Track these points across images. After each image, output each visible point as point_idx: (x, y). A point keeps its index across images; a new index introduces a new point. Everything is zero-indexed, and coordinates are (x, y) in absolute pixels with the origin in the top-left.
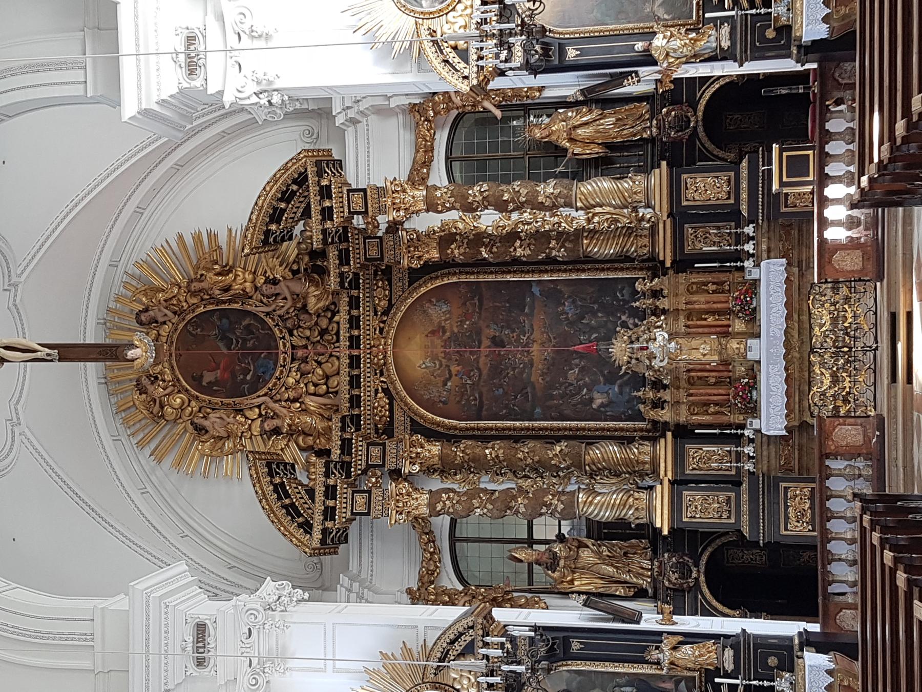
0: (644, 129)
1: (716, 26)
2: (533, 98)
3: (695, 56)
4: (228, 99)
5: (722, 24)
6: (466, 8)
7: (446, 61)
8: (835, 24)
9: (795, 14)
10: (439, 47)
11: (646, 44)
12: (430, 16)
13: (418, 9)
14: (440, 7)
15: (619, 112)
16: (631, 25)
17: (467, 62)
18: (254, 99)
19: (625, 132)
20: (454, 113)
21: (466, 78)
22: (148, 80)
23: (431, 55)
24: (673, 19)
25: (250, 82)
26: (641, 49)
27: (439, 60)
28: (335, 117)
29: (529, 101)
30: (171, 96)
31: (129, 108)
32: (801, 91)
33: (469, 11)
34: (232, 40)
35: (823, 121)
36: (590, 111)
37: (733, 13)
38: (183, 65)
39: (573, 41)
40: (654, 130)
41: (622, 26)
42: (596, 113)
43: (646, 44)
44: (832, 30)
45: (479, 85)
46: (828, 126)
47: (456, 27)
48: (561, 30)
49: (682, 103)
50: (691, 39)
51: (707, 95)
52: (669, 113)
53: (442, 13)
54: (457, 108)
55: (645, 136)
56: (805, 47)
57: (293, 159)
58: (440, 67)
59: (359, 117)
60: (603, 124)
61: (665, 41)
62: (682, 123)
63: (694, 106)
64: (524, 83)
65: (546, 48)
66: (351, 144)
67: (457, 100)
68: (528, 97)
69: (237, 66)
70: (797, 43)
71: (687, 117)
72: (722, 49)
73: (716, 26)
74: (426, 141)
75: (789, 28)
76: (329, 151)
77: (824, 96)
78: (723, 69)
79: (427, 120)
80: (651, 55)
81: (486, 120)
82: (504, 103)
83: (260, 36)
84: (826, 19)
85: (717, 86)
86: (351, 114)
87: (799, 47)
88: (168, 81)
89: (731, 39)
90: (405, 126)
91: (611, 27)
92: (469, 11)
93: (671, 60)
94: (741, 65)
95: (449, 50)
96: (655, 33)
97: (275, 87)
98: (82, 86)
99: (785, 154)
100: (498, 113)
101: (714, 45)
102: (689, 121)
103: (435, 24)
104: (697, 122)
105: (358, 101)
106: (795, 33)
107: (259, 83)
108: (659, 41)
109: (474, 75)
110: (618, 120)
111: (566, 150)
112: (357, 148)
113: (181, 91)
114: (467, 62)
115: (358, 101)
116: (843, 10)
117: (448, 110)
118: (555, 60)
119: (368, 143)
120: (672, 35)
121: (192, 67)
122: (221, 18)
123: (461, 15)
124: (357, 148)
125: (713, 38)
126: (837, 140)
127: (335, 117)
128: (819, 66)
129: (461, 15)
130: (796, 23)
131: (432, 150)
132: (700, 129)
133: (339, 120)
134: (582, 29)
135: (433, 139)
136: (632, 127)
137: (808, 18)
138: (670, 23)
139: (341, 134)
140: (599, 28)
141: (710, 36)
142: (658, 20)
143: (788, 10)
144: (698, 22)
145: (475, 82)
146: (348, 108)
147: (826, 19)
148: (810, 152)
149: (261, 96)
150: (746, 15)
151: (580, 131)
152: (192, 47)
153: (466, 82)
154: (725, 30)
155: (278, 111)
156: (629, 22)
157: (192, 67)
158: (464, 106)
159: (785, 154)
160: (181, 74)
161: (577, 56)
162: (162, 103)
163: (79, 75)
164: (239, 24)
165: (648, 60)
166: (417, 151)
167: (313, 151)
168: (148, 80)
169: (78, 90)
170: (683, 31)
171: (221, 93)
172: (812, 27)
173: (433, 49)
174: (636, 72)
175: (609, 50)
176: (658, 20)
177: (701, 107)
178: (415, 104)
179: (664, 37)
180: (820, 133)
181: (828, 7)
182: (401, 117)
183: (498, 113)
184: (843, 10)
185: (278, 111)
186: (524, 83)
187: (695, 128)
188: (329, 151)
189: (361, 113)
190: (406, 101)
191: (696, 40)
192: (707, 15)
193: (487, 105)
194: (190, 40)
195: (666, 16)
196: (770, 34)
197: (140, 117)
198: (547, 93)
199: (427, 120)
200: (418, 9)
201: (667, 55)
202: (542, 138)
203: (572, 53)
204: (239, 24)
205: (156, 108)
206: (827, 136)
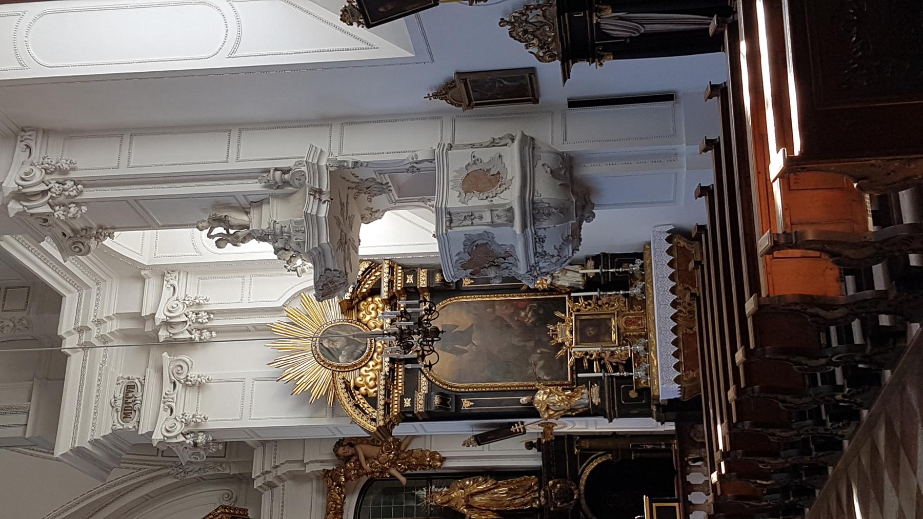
0: (534, 500)
1: (587, 386)
2: (435, 467)
3: (572, 410)
4: (157, 436)
5: (592, 384)
6: (377, 364)
7: (357, 406)
8: (686, 385)
9: (652, 378)
10: (352, 394)
11: (530, 398)
12: (345, 369)
13: (335, 364)
14: (354, 362)
15: (511, 483)
16: (517, 383)
17: (375, 407)
18: (182, 439)
19: (517, 501)
20: (365, 479)
21: (374, 420)
22: (86, 416)
23: (344, 400)
24: (552, 380)
25: (178, 425)
26: (525, 402)
27: (351, 404)
28: (254, 480)
29: (431, 471)
30: (104, 437)
31: (63, 446)
32: (663, 447)
33: (378, 367)
34: (168, 387)
35: (685, 473)
36: (486, 481)
37: (601, 374)
38: (120, 409)
39: (468, 395)
40: (542, 499)
41: (509, 384)
42: (490, 483)
43: (530, 398)
44: (683, 390)
45: (385, 426)
46: (689, 478)
47: (368, 378)
48: (457, 385)
49: (566, 477)
50: (567, 395)
51: (587, 472)
52: (554, 485)
53: (357, 367)
54: (367, 474)
55: (534, 506)
56: (663, 406)
57: (210, 514)
58: (351, 410)
59: (276, 482)
60: (496, 493)
61: (545, 397)
62: (566, 495)
63: (577, 479)
64: (425, 430)
65: (444, 397)
66: (266, 507)
67: (367, 467)
68: (430, 466)
69: (169, 410)
70: (656, 402)
71: (571, 489)
72: (593, 405)
73: (587, 386)
74: (337, 504)
75: (648, 390)
76: (245, 510)
77: (683, 452)
78: (596, 424)
79: (339, 485)
80: (534, 408)
81: (392, 489)
82: (409, 472)
83: (193, 385)
84: (677, 380)
85: (595, 464)
86: (269, 478)
87: (658, 406)
88: (106, 423)
89: (600, 397)
90: (317, 491)
91: (500, 384)
92: (378, 367)
93: (551, 413)
94: (611, 421)
95: (360, 397)
96: (537, 390)
97: (202, 428)
98: (25, 416)
99: (654, 505)
100: (403, 480)
101: (587, 401)
102: (573, 494)
103: (350, 376)
104: (579, 495)
105: (277, 467)
106: (654, 393)
107: (187, 425)
108: (540, 397)
109: (381, 418)
110: (510, 490)
111: (464, 515)
112: (272, 511)
113: (115, 432)
114: (375, 407)
115: (277, 467)
116: (692, 374)
117: (358, 476)
118: (452, 408)
119: (283, 506)
120: (551, 392)
121: (128, 409)
122: (160, 371)
123: (372, 370)
124: (272, 511)
125: (585, 396)
126: (698, 491)
127: (254, 480)
128: (677, 426)
129: (372, 370)
130: (653, 384)
131: (342, 513)
132: (583, 501)
133: (257, 484)
134: (475, 385)
135: (343, 503)
136: (523, 497)
137: (662, 378)
138: (549, 383)
139: (259, 495)
140: (490, 384)
141: (583, 394)
142: (539, 380)
143: (646, 374)
144: (573, 384)
145: (381, 423)
146: (268, 472)
147: (677, 380)
148: (676, 504)
149: (188, 436)
150: (612, 377)
151: (477, 499)
152: (130, 395)
153: (374, 423)
154: (595, 389)
155: (202, 452)
156: (515, 381)
157: (128, 409)
158: (373, 472)
159: (654, 505)
160: (117, 417)
161: (471, 406)
162: (94, 443)
163: (21, 419)
164: (176, 375)
165: (531, 412)
166: (328, 514)
167: (230, 508)
168: (86, 416)
169: (18, 432)
170: (560, 389)
171: (150, 434)
172: (667, 388)
173: (346, 395)
174: (522, 423)
175: (499, 403)
176: (539, 380)
177: (583, 482)
178: (328, 471)
179: (545, 393)
180: (683, 483)
181: (679, 371)
182: (314, 482)
183: (403, 480)
184: (692, 374)
185: (202, 452)
186: (425, 430)
187: (578, 500)
188: (245, 510)
189: (279, 478)
190: (320, 467)
191: (571, 397)
192: (579, 375)
193: (394, 471)
194: (130, 388)
195: (545, 378)
196: (633, 394)
197: (71, 454)
198: (448, 464)
199: (339, 485)
200: (335, 364)
201: (548, 408)
202: (443, 503)
203: (466, 404)
204: (176, 375)
205: (88, 446)
206: (689, 488)
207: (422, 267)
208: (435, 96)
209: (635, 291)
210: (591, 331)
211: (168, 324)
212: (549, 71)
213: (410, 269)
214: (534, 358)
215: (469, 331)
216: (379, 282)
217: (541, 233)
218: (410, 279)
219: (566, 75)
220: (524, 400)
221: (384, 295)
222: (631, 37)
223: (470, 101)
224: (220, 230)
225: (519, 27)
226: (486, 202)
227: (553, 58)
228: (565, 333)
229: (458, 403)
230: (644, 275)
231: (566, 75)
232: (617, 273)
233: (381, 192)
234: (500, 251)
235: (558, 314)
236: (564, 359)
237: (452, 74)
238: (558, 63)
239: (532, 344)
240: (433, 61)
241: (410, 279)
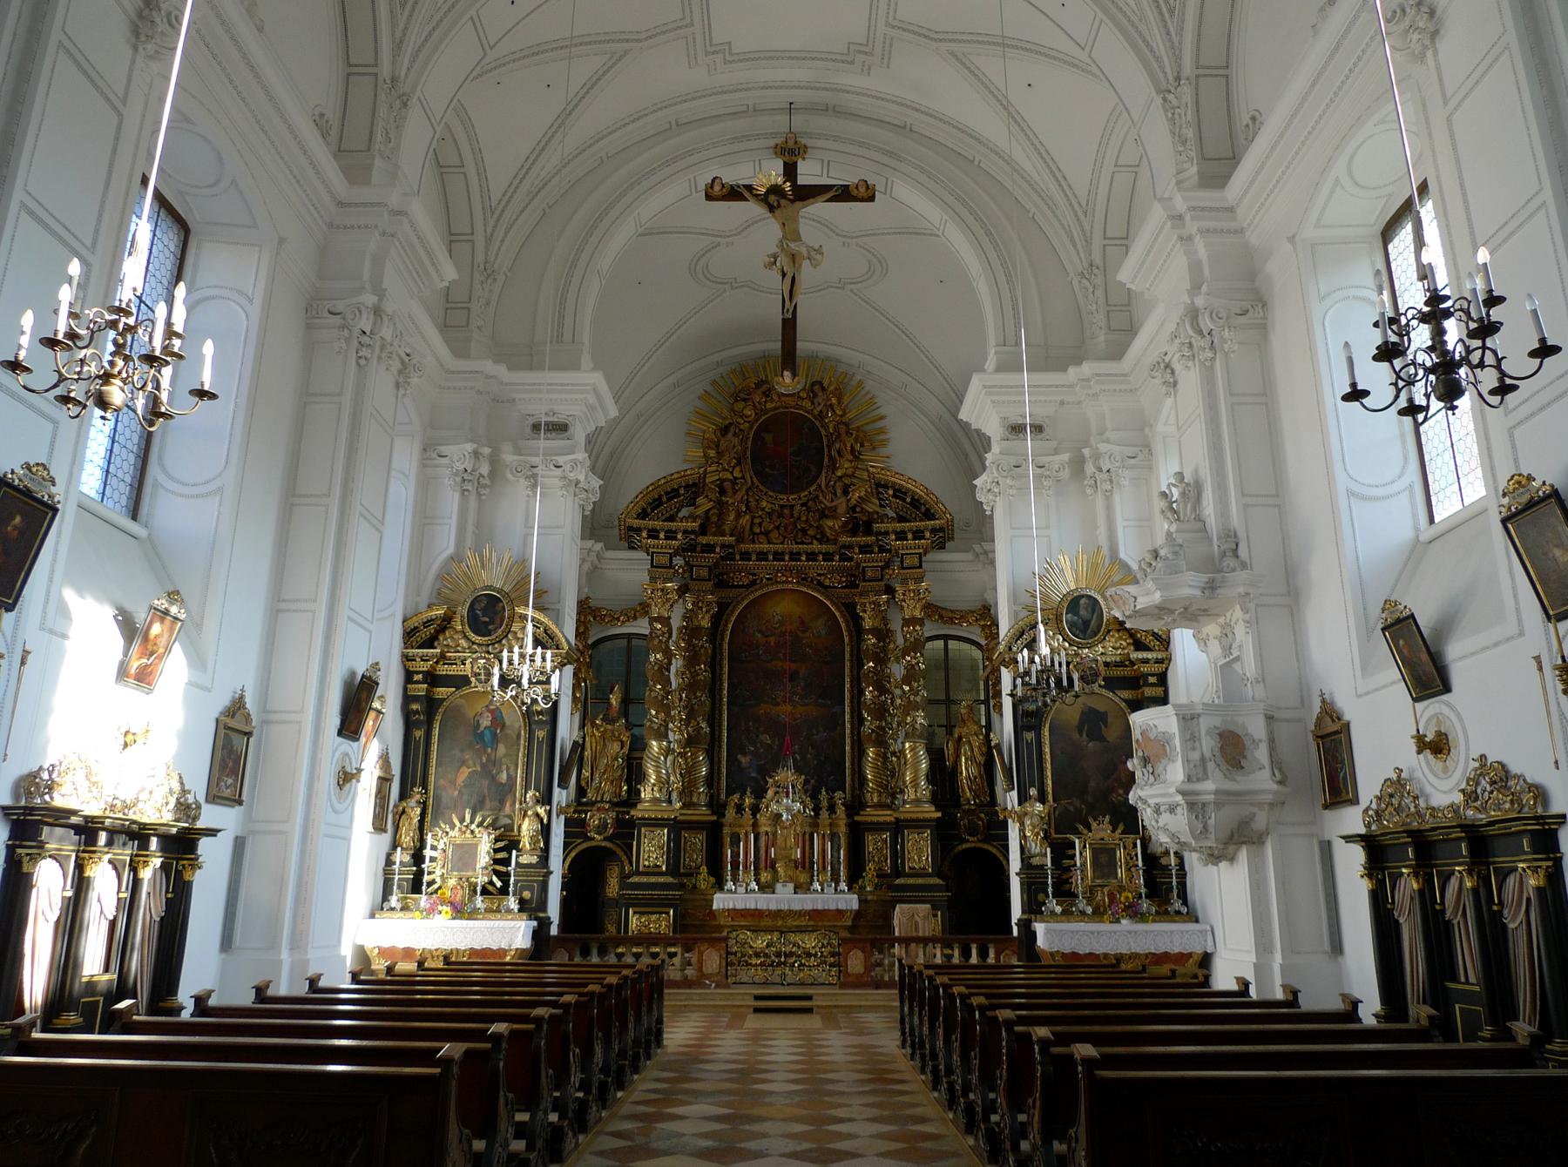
42: (981, 759)
51: (994, 851)
63: (986, 840)
108: (1039, 807)
165: (1023, 798)
207: (1166, 692)
208: (1323, 701)
209: (1145, 905)
210: (1103, 858)
211: (1097, 457)
212: (1352, 820)
213: (1162, 679)
214: (1077, 802)
215: (1102, 739)
216: (1148, 649)
217: (1179, 810)
218: (1152, 680)
219: (1348, 839)
220: (1033, 792)
221: (1135, 655)
222: (1443, 911)
223: (1322, 737)
224: (1176, 493)
225: (1397, 787)
226: (1208, 754)
227: (1368, 826)
228: (1102, 830)
229: (1029, 729)
230: (1163, 914)
231: (1348, 839)
232: (1164, 888)
233: (1223, 648)
234: (1159, 770)
235: (1121, 828)
236: (1077, 833)
237: (1347, 717)
238: (1363, 831)
239: (1090, 799)
240: (1359, 696)
241: (1152, 680)
